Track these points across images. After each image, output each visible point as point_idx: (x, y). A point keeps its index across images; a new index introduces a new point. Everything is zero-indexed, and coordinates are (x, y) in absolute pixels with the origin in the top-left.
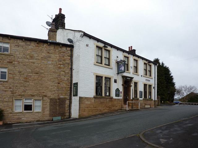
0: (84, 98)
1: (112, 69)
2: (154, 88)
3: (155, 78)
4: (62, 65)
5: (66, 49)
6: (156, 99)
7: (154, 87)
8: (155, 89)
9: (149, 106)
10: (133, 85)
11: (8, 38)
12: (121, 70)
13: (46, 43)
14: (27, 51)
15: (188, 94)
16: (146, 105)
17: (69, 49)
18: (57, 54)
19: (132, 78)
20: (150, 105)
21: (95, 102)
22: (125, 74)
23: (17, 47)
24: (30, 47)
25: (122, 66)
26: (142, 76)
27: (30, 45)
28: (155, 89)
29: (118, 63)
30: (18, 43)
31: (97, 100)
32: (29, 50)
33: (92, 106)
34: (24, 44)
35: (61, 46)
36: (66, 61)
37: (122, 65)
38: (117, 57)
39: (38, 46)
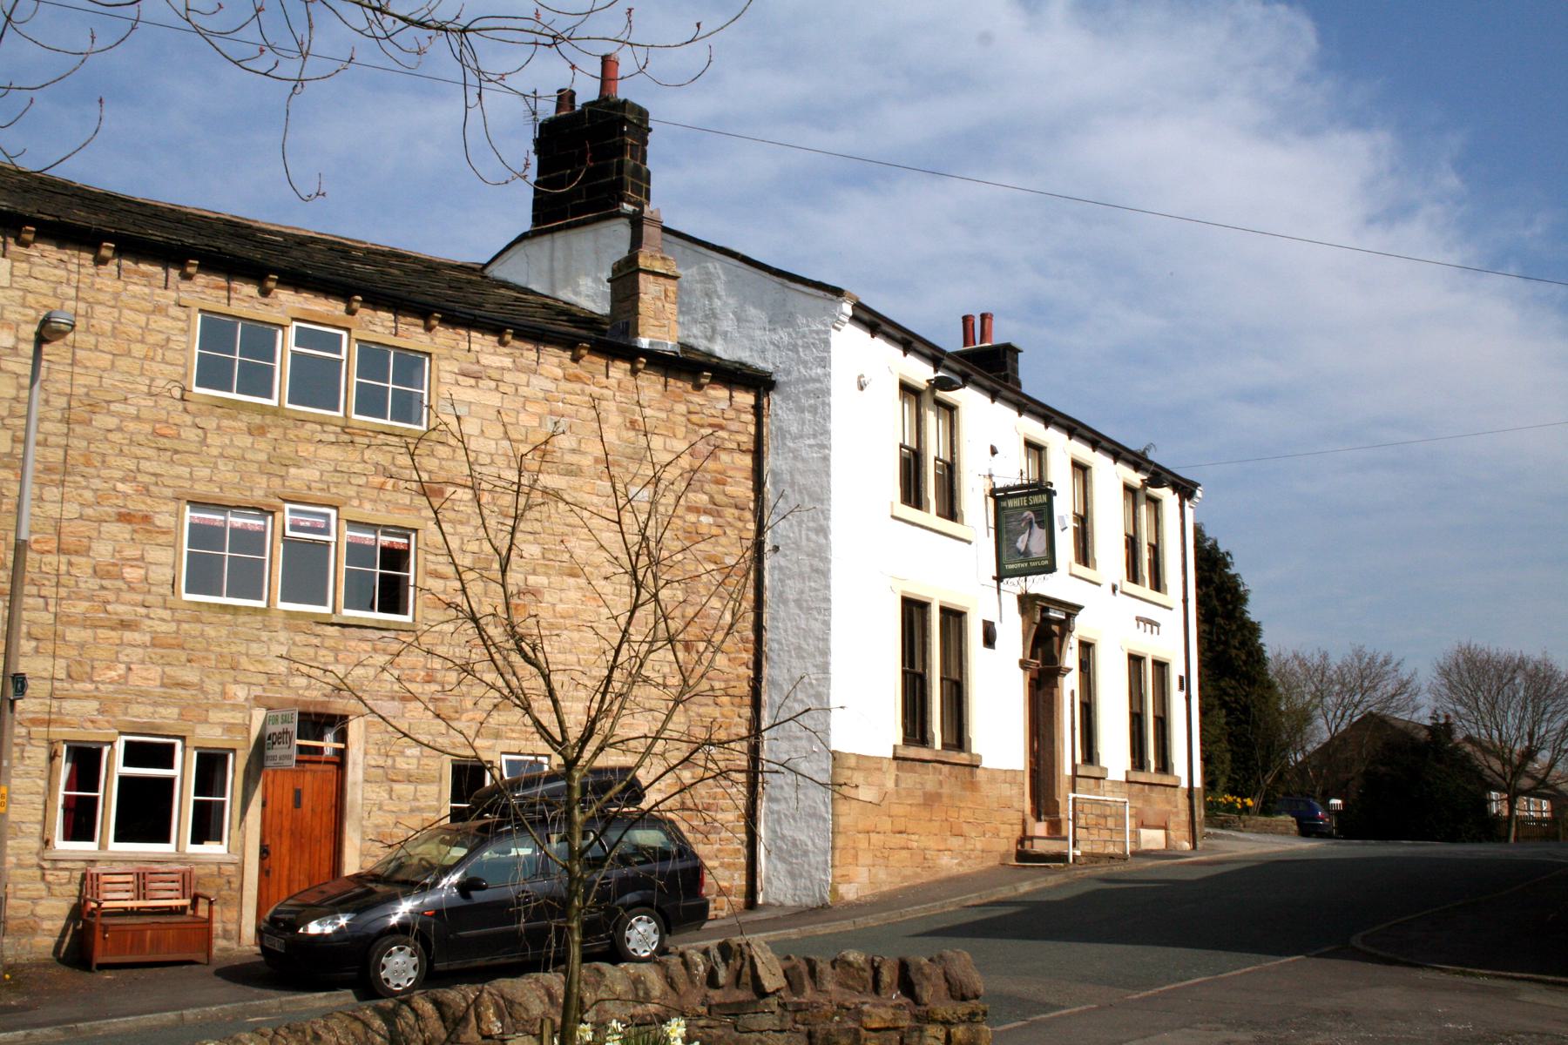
0: (852, 762)
1: (970, 543)
2: (1181, 688)
3: (1185, 601)
4: (706, 512)
5: (731, 397)
6: (1198, 783)
7: (1181, 678)
8: (1188, 698)
9: (1161, 833)
10: (1468, 748)
11: (19, 231)
12: (1027, 553)
13: (624, 359)
14: (523, 417)
15: (1343, 727)
16: (1143, 826)
17: (746, 399)
18: (681, 431)
19: (1072, 609)
20: (1166, 828)
21: (897, 792)
22: (1039, 585)
23: (472, 381)
24: (539, 384)
25: (1030, 524)
26: (1114, 588)
27: (535, 372)
28: (1188, 698)
29: (999, 496)
30: (472, 356)
31: (910, 779)
32: (531, 408)
33: (886, 825)
34: (508, 362)
35: (29, 232)
36: (728, 489)
37: (1028, 514)
38: (994, 451)
39: (578, 379)
